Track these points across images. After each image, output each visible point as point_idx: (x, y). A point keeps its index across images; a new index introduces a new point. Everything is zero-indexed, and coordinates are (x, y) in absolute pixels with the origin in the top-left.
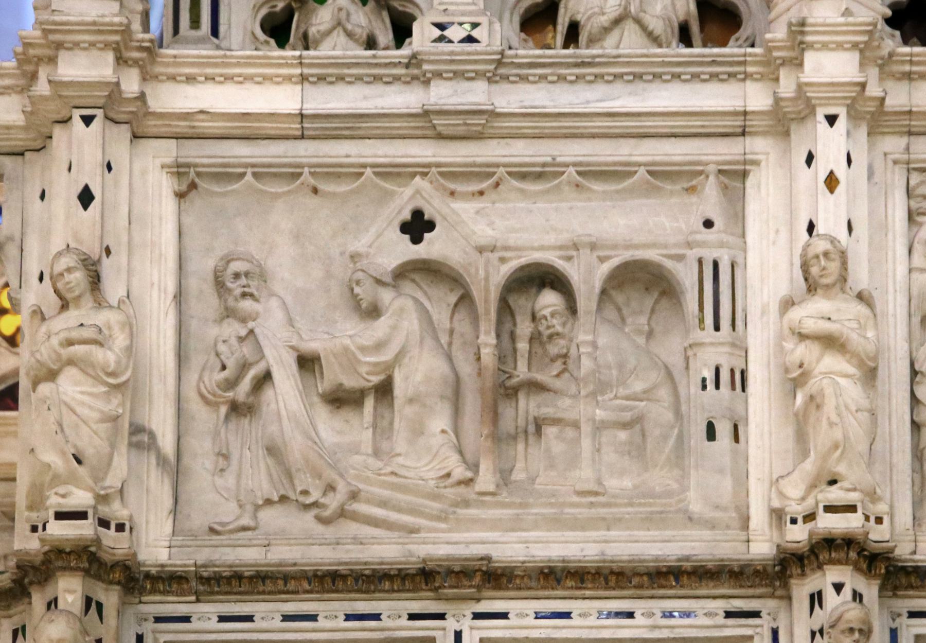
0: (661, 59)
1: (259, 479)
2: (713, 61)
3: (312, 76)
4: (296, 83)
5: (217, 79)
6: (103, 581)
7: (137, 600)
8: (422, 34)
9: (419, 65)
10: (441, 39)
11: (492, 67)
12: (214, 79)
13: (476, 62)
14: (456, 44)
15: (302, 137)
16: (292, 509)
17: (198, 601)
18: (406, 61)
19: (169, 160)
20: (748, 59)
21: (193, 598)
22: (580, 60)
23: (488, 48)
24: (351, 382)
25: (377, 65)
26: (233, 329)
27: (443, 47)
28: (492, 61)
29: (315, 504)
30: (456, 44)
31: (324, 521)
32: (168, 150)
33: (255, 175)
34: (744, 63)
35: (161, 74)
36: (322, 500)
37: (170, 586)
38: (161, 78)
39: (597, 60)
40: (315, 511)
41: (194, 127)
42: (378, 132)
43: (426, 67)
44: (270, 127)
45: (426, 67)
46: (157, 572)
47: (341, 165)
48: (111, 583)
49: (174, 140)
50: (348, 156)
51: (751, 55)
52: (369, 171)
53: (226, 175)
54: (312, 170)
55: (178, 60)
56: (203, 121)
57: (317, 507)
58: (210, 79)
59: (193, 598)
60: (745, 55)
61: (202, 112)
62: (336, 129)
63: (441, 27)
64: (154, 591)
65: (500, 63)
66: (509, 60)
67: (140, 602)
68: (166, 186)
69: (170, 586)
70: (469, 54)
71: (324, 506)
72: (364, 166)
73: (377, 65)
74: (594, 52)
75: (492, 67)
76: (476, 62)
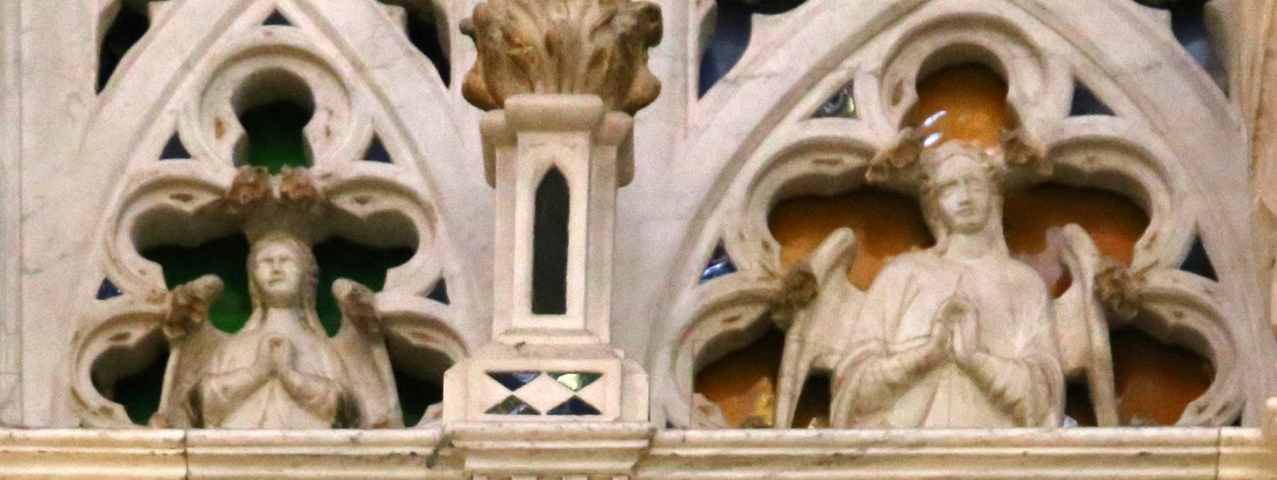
0: (1019, 451)
2: (1142, 454)
8: (465, 398)
9: (457, 459)
10: (509, 406)
11: (627, 465)
13: (589, 454)
14: (544, 417)
18: (428, 451)
20: (1224, 450)
22: (830, 452)
23: (619, 426)
25: (359, 460)
27: (515, 422)
28: (627, 453)
30: (544, 417)
34: (1215, 459)
39: (872, 451)
43: (472, 464)
45: (472, 464)
51: (1230, 442)
60: (1217, 443)
63: (510, 380)
65: (644, 457)
66: (667, 452)
70: (573, 437)
73: (359, 460)
74: (865, 434)
75: (627, 465)
76: (589, 454)
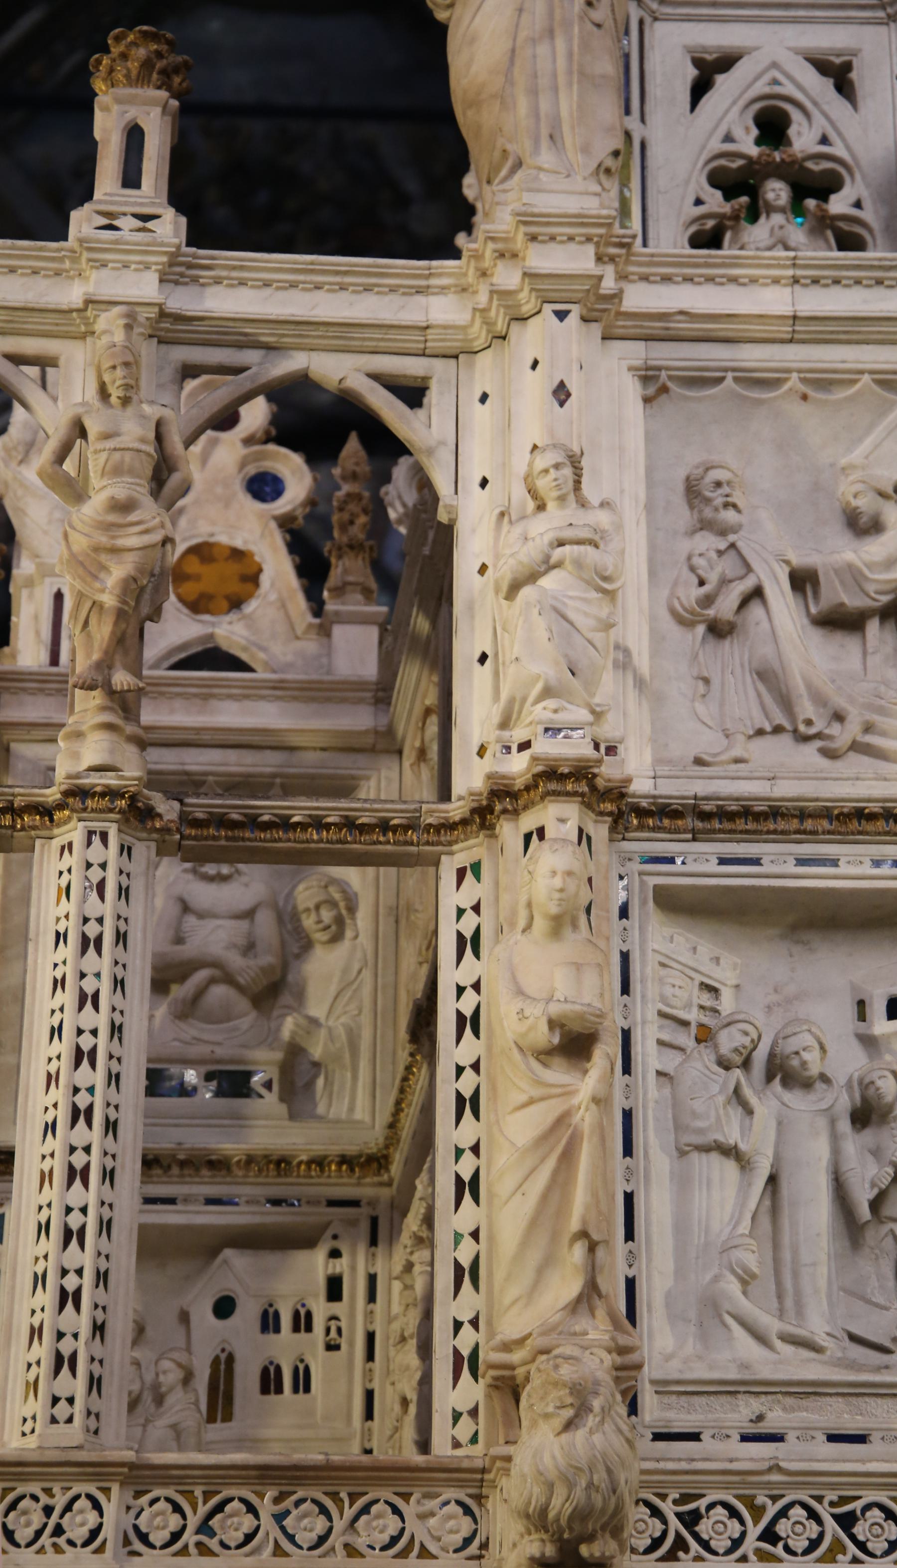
1: (747, 705)
3: (805, 277)
4: (785, 285)
5: (696, 279)
6: (593, 811)
7: (621, 836)
12: (692, 280)
15: (791, 341)
16: (786, 740)
17: (694, 839)
19: (638, 363)
21: (690, 836)
24: (853, 601)
26: (708, 542)
29: (818, 736)
31: (830, 754)
32: (637, 352)
33: (736, 379)
35: (633, 274)
36: (827, 731)
37: (661, 820)
38: (631, 277)
40: (819, 744)
41: (667, 329)
42: (880, 337)
44: (755, 329)
46: (649, 803)
47: (835, 371)
48: (601, 814)
49: (643, 343)
50: (843, 362)
52: (866, 377)
53: (701, 380)
54: (802, 375)
55: (655, 259)
56: (679, 322)
57: (820, 739)
58: (688, 279)
59: (690, 836)
61: (681, 313)
62: (832, 332)
64: (641, 827)
67: (624, 839)
68: (633, 390)
69: (661, 820)
71: (830, 737)
72: (862, 372)
